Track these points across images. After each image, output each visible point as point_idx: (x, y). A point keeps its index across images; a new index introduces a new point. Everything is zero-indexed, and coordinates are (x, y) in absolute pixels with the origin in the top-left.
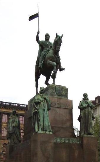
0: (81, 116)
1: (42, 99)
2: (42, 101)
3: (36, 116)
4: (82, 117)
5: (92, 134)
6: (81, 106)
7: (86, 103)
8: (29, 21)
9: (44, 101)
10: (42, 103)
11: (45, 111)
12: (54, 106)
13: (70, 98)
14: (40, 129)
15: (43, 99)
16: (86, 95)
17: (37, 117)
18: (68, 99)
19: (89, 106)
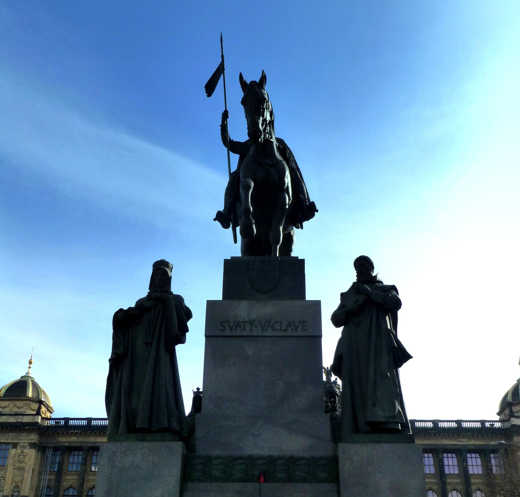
3: (119, 374)
12: (234, 333)
13: (310, 295)
18: (306, 300)
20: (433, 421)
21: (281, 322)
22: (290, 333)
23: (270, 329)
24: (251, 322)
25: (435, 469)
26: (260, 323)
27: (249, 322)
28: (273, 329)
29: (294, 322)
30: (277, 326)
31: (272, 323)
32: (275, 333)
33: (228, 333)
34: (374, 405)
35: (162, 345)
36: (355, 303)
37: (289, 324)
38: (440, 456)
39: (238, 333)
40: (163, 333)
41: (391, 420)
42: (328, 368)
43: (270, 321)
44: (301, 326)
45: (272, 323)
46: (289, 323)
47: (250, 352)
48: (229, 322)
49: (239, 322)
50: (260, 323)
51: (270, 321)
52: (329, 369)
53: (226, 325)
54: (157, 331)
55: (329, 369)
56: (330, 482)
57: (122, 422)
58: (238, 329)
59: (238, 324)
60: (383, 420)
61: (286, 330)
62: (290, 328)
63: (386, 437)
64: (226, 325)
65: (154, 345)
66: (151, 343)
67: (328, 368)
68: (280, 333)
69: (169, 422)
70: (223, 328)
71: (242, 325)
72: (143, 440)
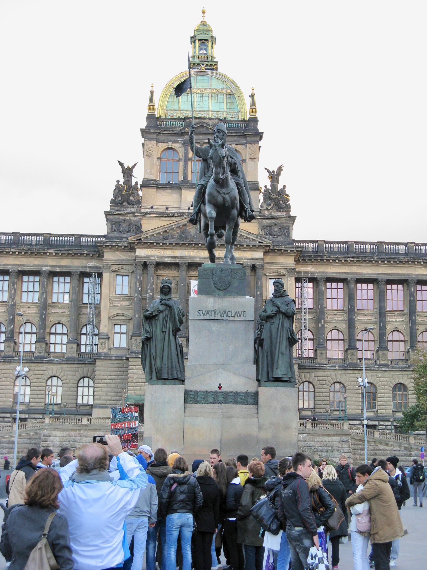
0: (262, 338)
1: (161, 308)
2: (162, 312)
3: (149, 348)
4: (263, 339)
5: (283, 379)
6: (263, 314)
7: (274, 305)
8: (177, 97)
9: (164, 312)
10: (161, 315)
11: (167, 333)
14: (154, 373)
15: (164, 307)
16: (278, 284)
17: (150, 345)
19: (279, 311)
20: (406, 244)
21: (232, 311)
22: (236, 318)
23: (225, 315)
24: (215, 311)
25: (405, 305)
26: (220, 311)
27: (214, 311)
28: (227, 315)
29: (238, 312)
30: (229, 314)
31: (226, 312)
32: (228, 318)
33: (202, 317)
34: (277, 369)
35: (171, 333)
36: (272, 312)
37: (236, 313)
38: (412, 289)
39: (207, 317)
40: (171, 326)
41: (284, 376)
42: (273, 172)
43: (225, 310)
44: (242, 314)
45: (226, 312)
46: (236, 312)
47: (214, 329)
48: (202, 311)
49: (208, 311)
50: (220, 311)
51: (225, 310)
52: (275, 173)
53: (201, 312)
54: (168, 325)
55: (275, 173)
56: (254, 404)
57: (154, 373)
58: (208, 315)
59: (208, 313)
60: (281, 376)
61: (234, 316)
62: (236, 315)
63: (282, 384)
64: (201, 312)
65: (167, 333)
66: (165, 332)
67: (273, 172)
68: (231, 318)
69: (177, 375)
70: (199, 314)
71: (210, 312)
72: (165, 384)
